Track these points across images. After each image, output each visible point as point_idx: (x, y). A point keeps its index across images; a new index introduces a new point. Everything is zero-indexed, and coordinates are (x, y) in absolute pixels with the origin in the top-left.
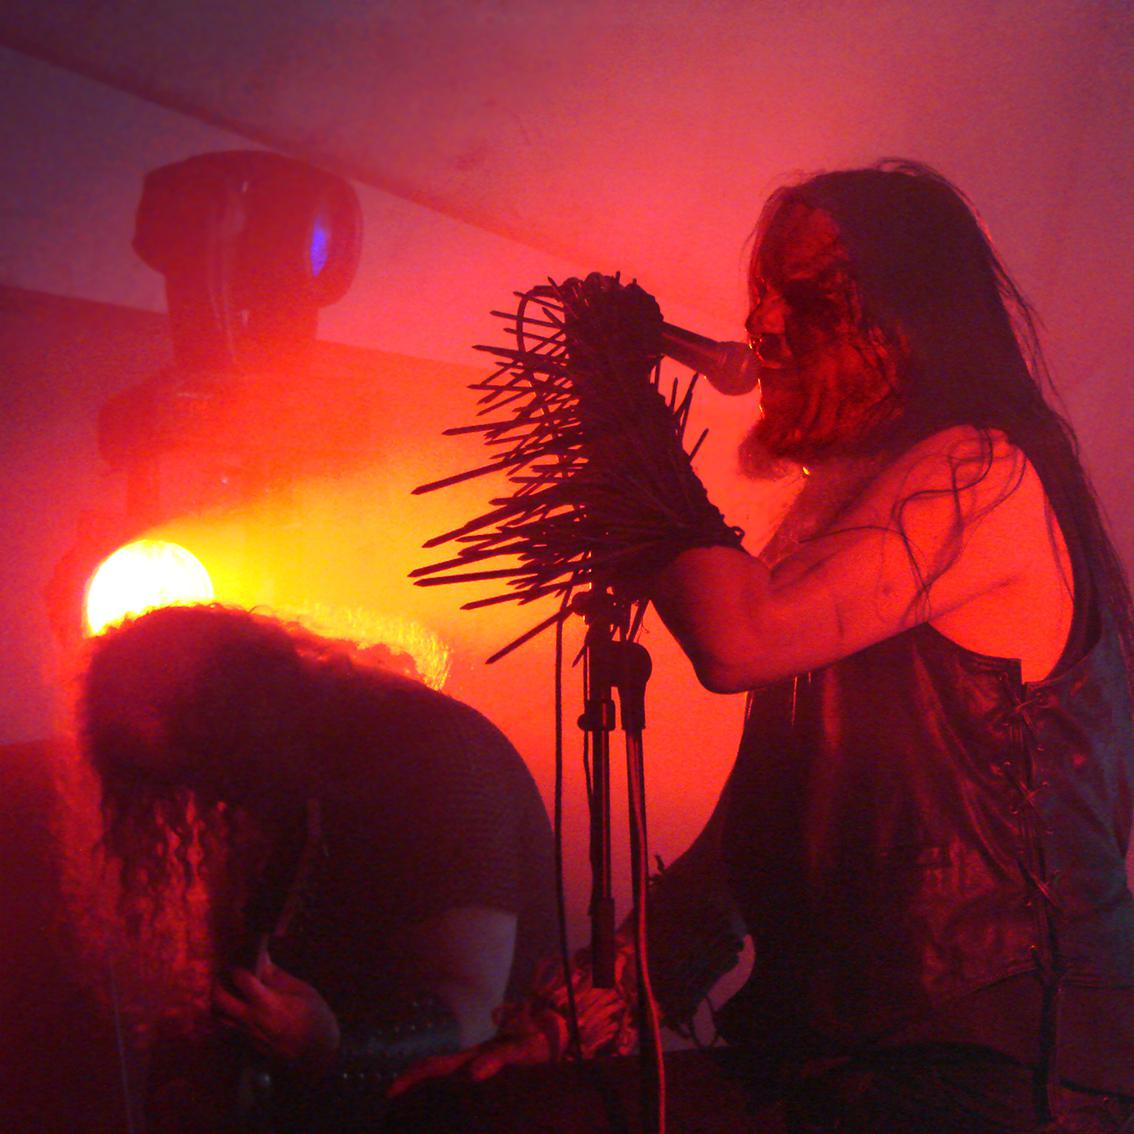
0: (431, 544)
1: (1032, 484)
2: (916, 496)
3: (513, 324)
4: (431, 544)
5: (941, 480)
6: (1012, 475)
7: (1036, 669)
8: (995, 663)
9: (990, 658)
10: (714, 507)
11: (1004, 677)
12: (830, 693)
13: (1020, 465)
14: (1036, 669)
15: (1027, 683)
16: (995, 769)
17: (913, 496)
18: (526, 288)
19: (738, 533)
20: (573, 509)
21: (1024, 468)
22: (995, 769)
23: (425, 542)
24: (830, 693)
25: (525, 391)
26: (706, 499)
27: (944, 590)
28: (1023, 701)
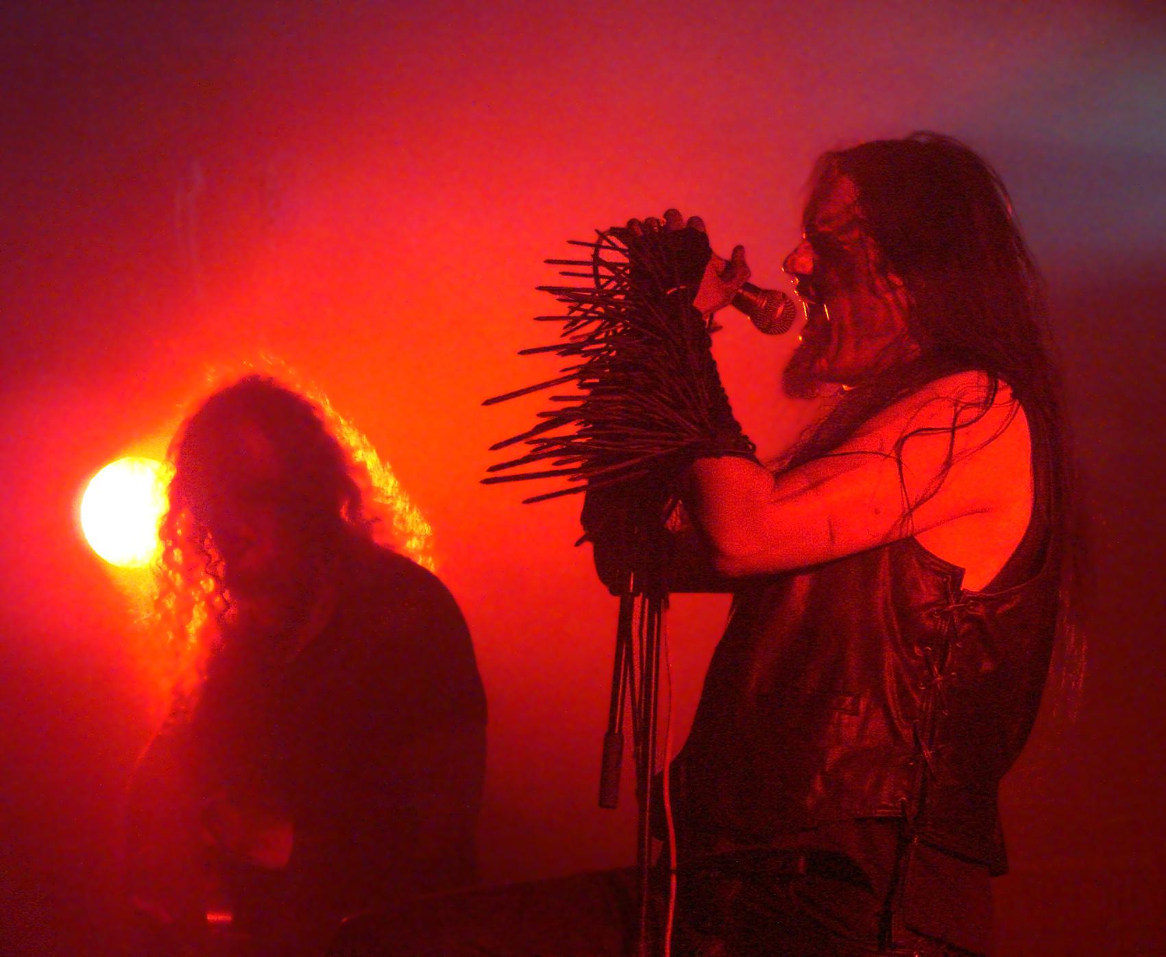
0: (496, 447)
1: (1021, 426)
2: (919, 432)
3: (588, 270)
4: (496, 447)
5: (944, 417)
6: (1011, 411)
7: (973, 583)
8: (944, 566)
9: (940, 560)
10: (737, 422)
11: (948, 579)
12: (802, 585)
13: (1016, 406)
14: (973, 583)
15: (964, 590)
16: (917, 649)
17: (917, 431)
18: (604, 228)
19: (751, 447)
20: (672, 868)
21: (1017, 408)
22: (917, 649)
23: (491, 446)
24: (802, 585)
25: (591, 320)
26: (731, 415)
27: (920, 517)
28: (957, 602)
